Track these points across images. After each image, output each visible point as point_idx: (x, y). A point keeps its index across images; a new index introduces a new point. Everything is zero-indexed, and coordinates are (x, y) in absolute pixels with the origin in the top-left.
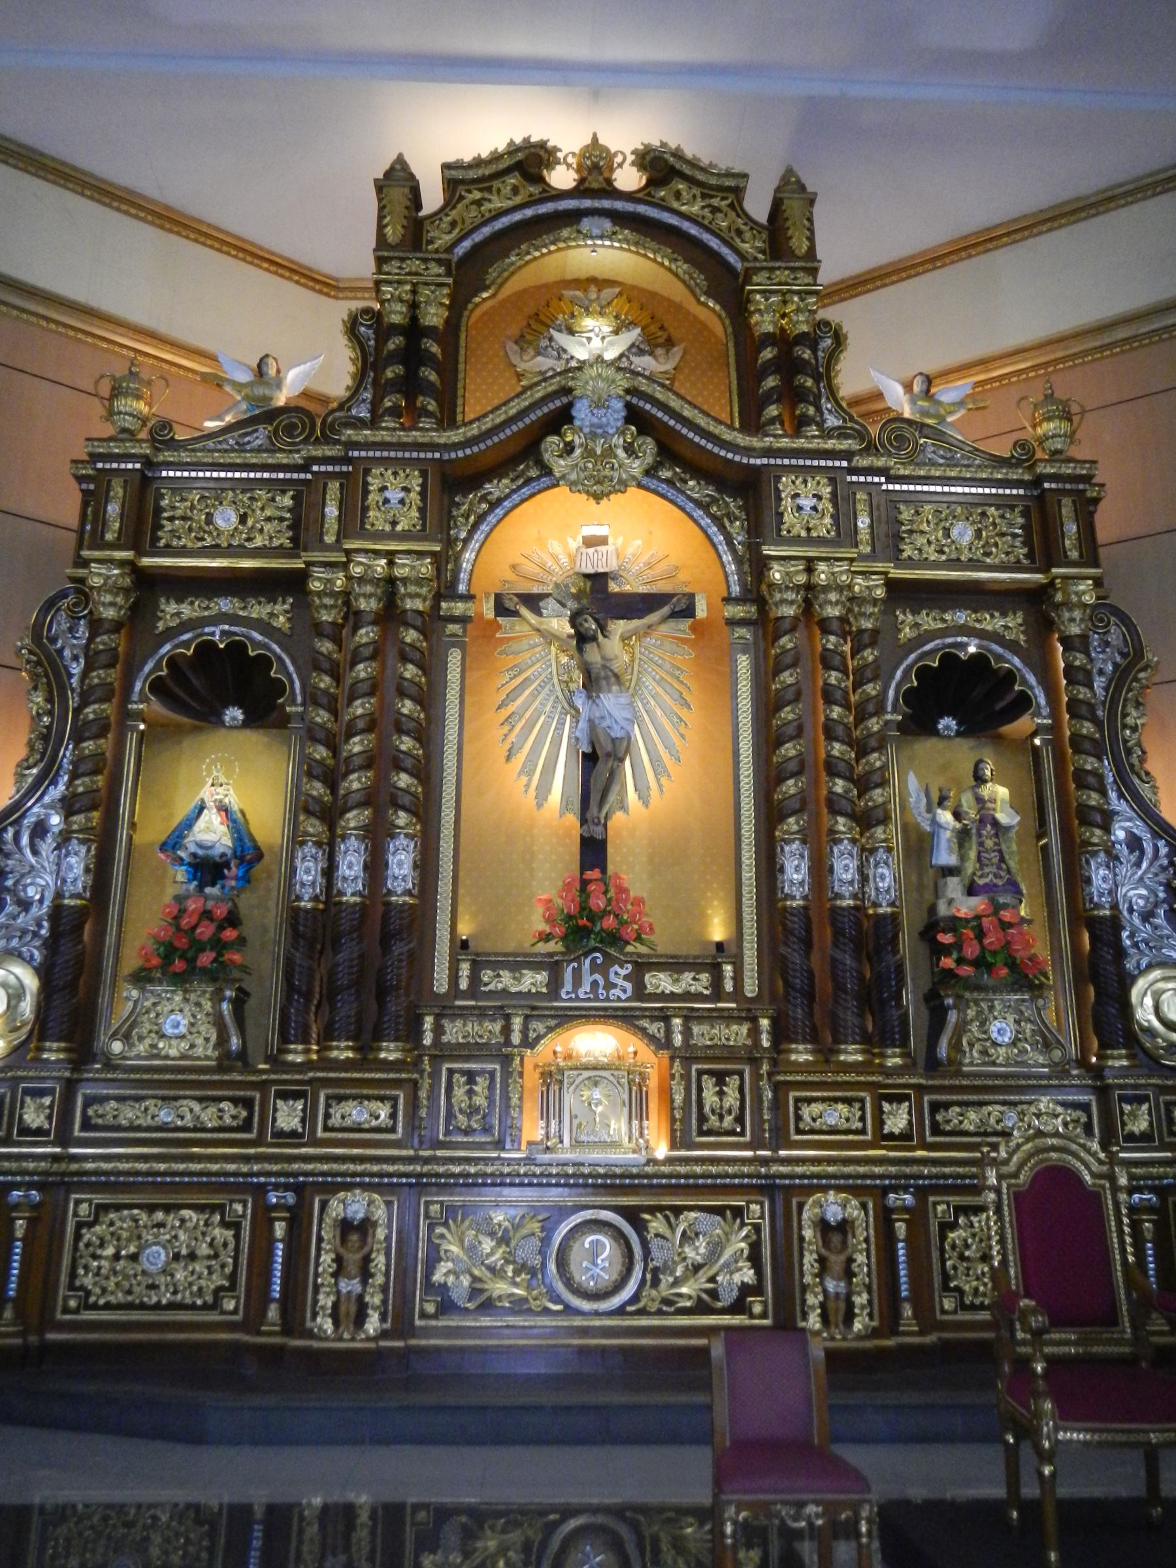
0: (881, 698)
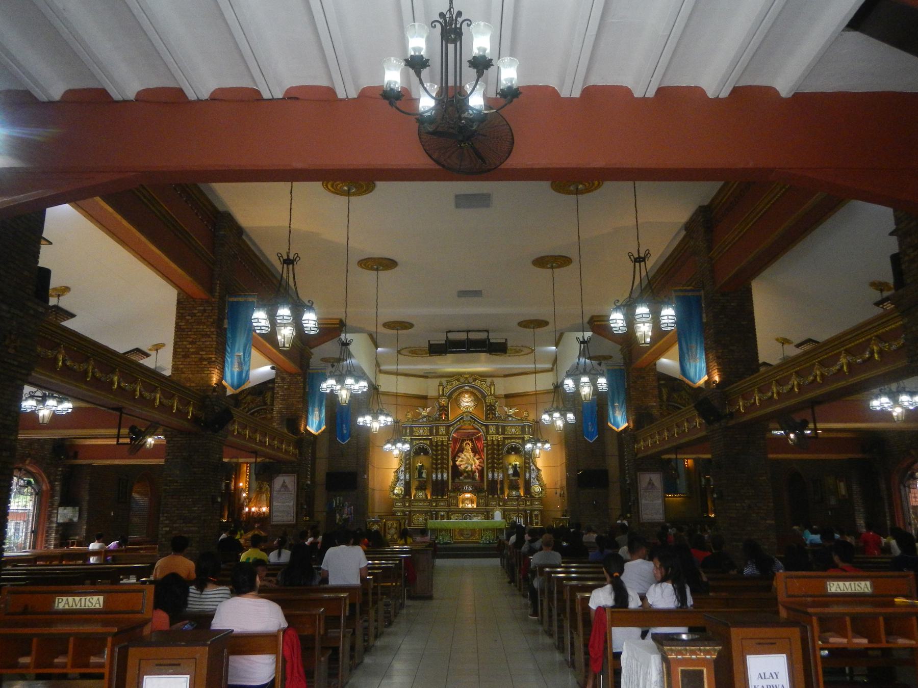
0: (502, 452)
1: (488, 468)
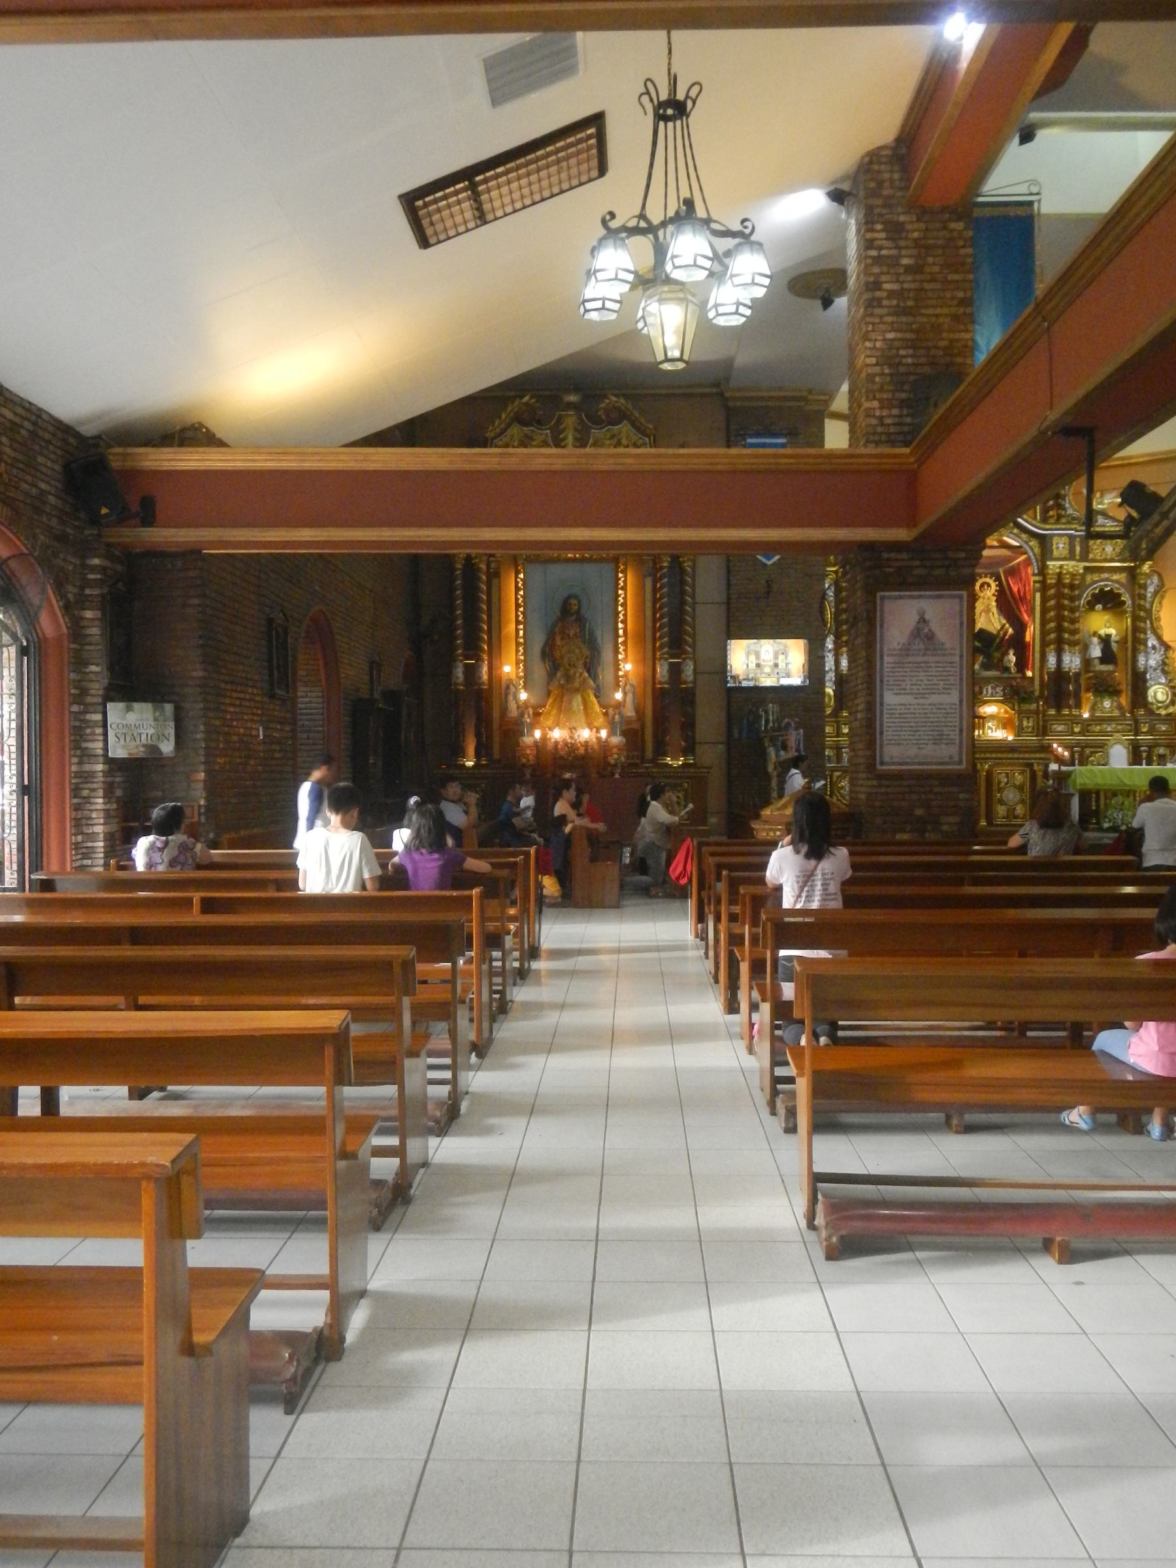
1: (1044, 644)
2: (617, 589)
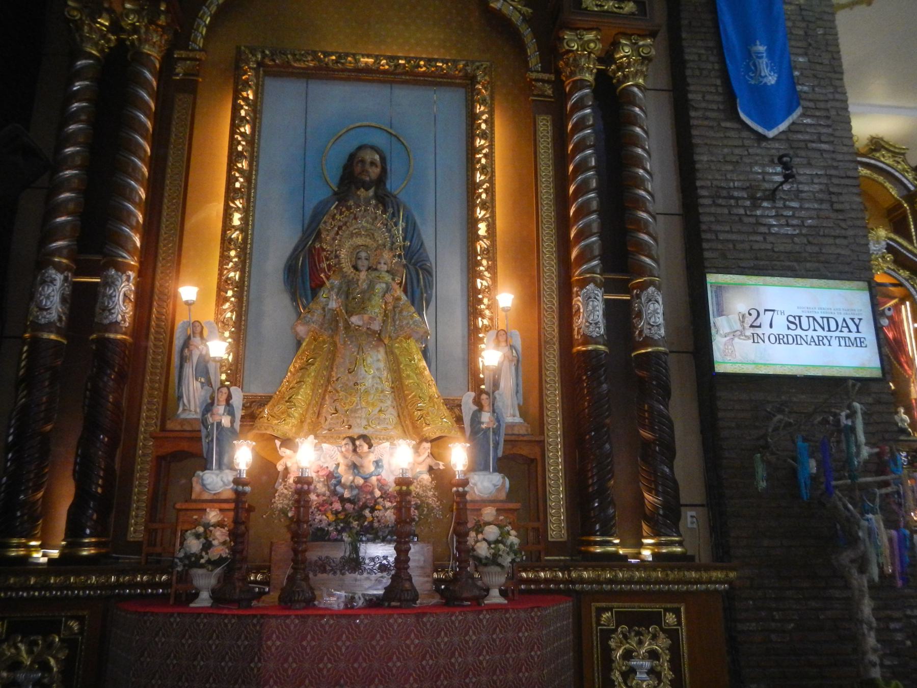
2: (471, 138)
